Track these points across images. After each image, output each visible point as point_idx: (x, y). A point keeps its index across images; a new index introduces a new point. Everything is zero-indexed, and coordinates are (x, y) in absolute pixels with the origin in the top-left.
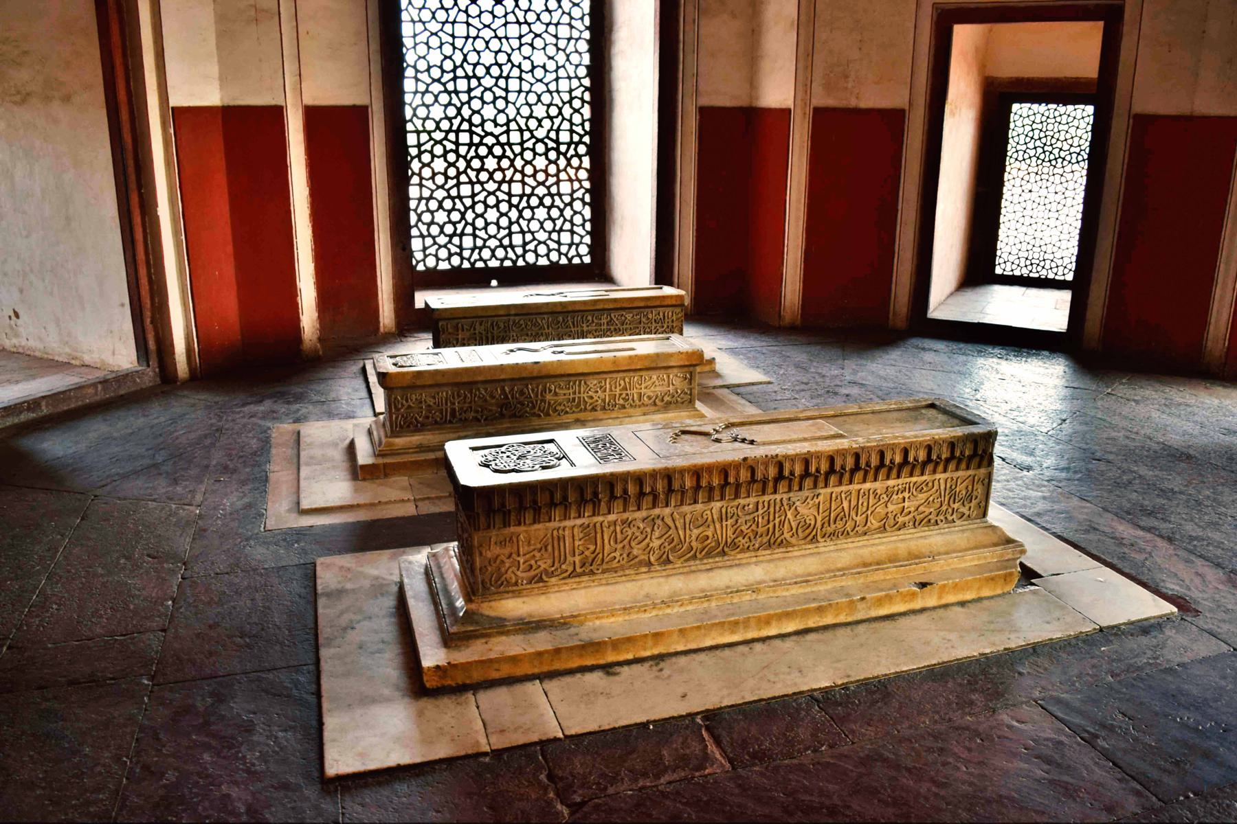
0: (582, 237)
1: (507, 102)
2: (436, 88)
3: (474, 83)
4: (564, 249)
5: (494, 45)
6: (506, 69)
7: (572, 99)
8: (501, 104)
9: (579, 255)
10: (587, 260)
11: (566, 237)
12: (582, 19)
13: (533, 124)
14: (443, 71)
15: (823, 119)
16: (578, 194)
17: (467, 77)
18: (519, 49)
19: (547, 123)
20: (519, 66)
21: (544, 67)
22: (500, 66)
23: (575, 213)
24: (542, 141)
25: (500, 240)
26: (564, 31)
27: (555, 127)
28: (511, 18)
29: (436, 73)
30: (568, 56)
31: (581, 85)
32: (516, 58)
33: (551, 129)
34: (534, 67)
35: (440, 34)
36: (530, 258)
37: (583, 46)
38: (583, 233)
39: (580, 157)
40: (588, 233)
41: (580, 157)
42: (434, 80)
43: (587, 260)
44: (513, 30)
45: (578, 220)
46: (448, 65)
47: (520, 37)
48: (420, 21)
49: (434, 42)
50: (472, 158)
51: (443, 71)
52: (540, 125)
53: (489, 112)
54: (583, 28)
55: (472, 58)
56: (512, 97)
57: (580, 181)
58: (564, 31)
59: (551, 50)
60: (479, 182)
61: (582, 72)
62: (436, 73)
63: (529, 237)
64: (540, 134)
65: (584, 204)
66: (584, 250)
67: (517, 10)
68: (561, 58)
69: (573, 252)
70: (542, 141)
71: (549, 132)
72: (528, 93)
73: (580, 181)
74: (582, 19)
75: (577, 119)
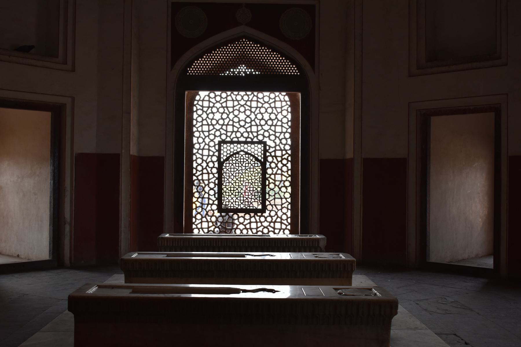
15: (371, 165)
16: (285, 205)
26: (278, 129)
31: (287, 153)
37: (287, 135)
39: (286, 187)
40: (289, 224)
41: (286, 187)
45: (284, 217)
57: (286, 199)
58: (278, 129)
63: (259, 224)
65: (288, 209)
73: (286, 199)
74: (287, 123)
75: (285, 169)
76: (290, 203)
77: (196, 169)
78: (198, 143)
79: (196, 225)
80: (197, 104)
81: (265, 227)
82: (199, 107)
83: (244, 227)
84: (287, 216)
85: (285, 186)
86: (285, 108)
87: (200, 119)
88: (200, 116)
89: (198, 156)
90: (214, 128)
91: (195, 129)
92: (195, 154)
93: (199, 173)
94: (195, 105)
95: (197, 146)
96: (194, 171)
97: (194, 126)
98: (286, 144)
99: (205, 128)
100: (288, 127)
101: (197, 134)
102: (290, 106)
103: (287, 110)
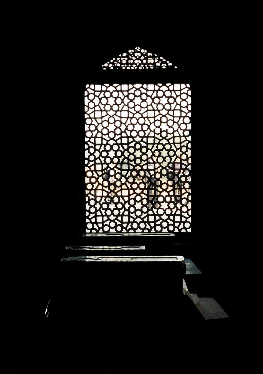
0: (187, 218)
1: (147, 149)
2: (112, 142)
3: (131, 140)
4: (177, 224)
5: (141, 121)
6: (147, 133)
7: (181, 147)
8: (144, 150)
9: (184, 228)
10: (189, 230)
11: (178, 218)
12: (187, 107)
13: (160, 160)
14: (115, 134)
17: (128, 137)
18: (154, 123)
19: (168, 159)
20: (154, 131)
21: (166, 131)
22: (144, 131)
23: (183, 205)
24: (165, 168)
25: (142, 219)
27: (172, 161)
28: (150, 108)
29: (112, 135)
30: (179, 126)
31: (186, 140)
32: (152, 127)
33: (170, 162)
34: (161, 132)
35: (115, 116)
36: (158, 228)
37: (187, 120)
38: (187, 216)
40: (190, 216)
42: (111, 139)
43: (189, 230)
44: (151, 114)
46: (118, 131)
47: (155, 117)
48: (105, 110)
49: (112, 120)
50: (129, 177)
51: (115, 134)
52: (164, 160)
53: (138, 154)
54: (187, 111)
55: (130, 127)
56: (150, 147)
58: (177, 113)
59: (171, 123)
60: (132, 189)
61: (187, 133)
62: (112, 135)
64: (164, 165)
66: (187, 225)
67: (153, 104)
68: (176, 127)
69: (181, 226)
70: (165, 168)
71: (169, 163)
72: (158, 144)
74: (187, 107)
75: (184, 157)
76: (189, 194)
77: (88, 159)
78: (90, 130)
79: (90, 219)
80: (89, 88)
81: (164, 221)
82: (90, 91)
83: (141, 220)
84: (187, 207)
85: (184, 175)
86: (185, 91)
87: (91, 105)
88: (91, 101)
89: (91, 145)
90: (108, 114)
91: (86, 116)
92: (86, 143)
93: (91, 163)
94: (86, 89)
95: (89, 134)
96: (86, 162)
97: (86, 113)
98: (186, 130)
99: (98, 114)
100: (187, 111)
101: (88, 121)
102: (190, 89)
103: (187, 94)
